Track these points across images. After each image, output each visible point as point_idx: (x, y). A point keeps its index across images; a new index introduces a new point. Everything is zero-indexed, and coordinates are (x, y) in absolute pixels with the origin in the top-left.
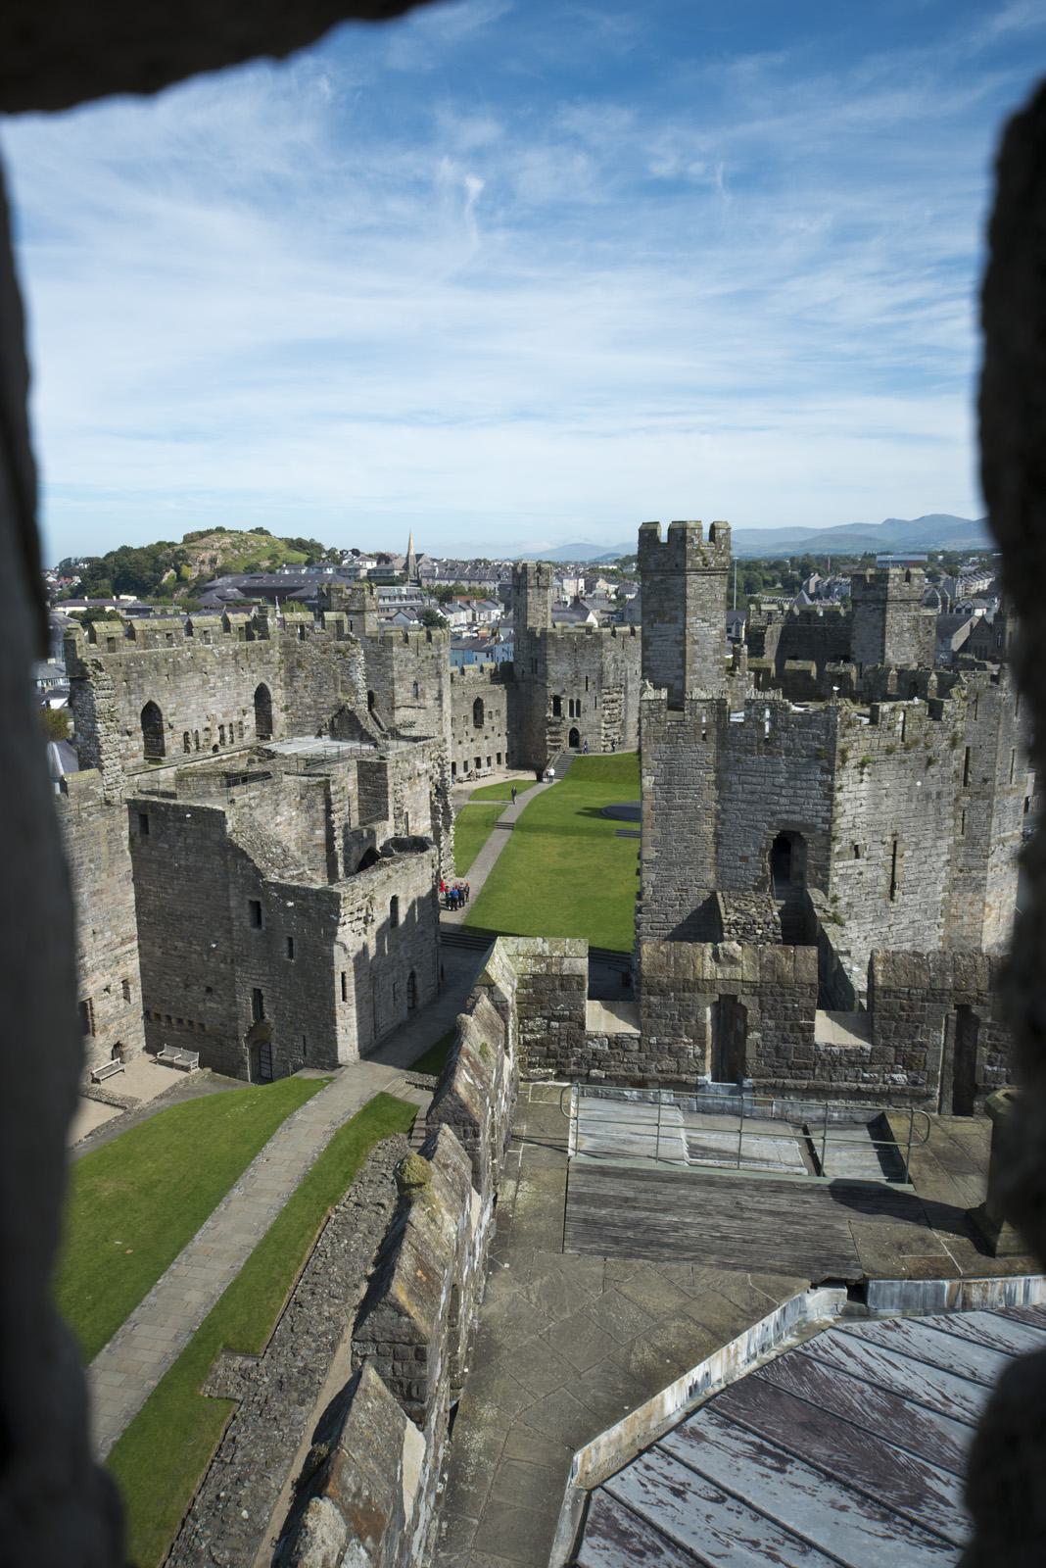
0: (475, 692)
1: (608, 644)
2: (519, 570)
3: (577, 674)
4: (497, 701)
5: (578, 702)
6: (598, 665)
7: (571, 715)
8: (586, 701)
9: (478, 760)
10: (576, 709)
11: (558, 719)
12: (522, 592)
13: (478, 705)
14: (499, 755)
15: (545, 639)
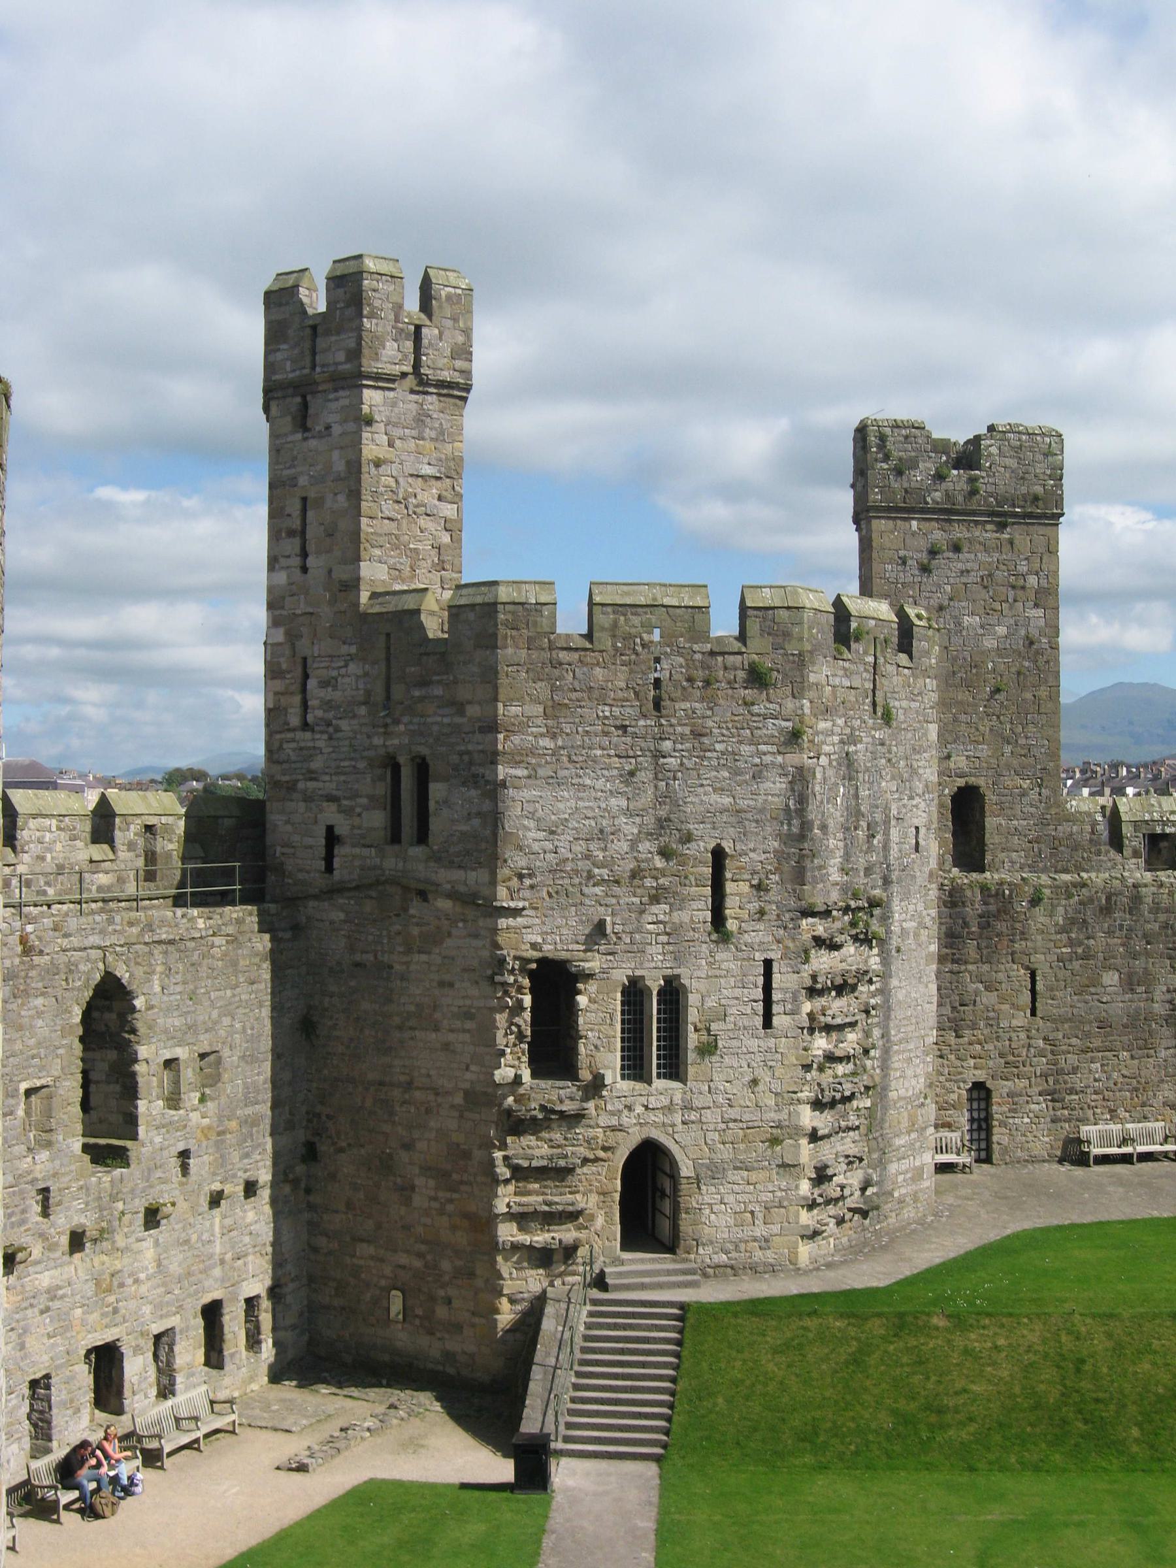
0: (86, 946)
1: (822, 672)
2: (317, 301)
3: (668, 832)
4: (212, 997)
5: (673, 993)
6: (775, 787)
7: (635, 1067)
8: (717, 987)
9: (106, 1361)
10: (660, 1032)
11: (558, 1093)
12: (328, 411)
13: (108, 1018)
14: (212, 1313)
15: (489, 641)
